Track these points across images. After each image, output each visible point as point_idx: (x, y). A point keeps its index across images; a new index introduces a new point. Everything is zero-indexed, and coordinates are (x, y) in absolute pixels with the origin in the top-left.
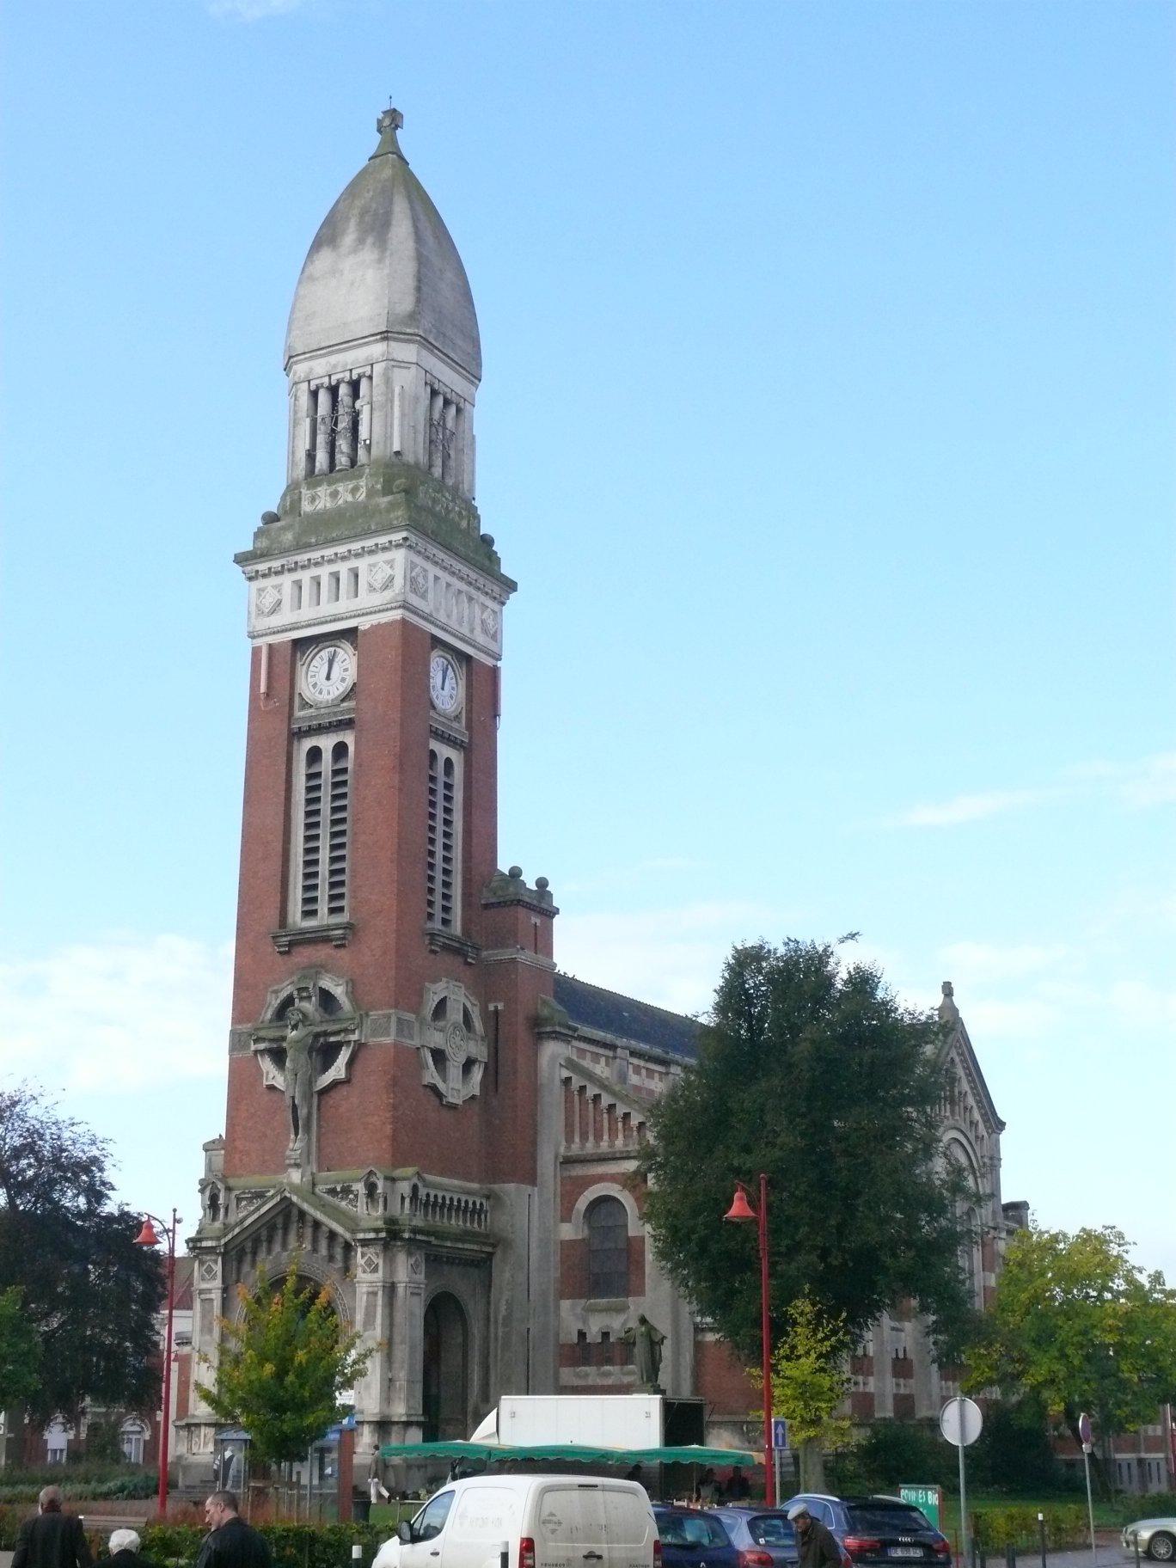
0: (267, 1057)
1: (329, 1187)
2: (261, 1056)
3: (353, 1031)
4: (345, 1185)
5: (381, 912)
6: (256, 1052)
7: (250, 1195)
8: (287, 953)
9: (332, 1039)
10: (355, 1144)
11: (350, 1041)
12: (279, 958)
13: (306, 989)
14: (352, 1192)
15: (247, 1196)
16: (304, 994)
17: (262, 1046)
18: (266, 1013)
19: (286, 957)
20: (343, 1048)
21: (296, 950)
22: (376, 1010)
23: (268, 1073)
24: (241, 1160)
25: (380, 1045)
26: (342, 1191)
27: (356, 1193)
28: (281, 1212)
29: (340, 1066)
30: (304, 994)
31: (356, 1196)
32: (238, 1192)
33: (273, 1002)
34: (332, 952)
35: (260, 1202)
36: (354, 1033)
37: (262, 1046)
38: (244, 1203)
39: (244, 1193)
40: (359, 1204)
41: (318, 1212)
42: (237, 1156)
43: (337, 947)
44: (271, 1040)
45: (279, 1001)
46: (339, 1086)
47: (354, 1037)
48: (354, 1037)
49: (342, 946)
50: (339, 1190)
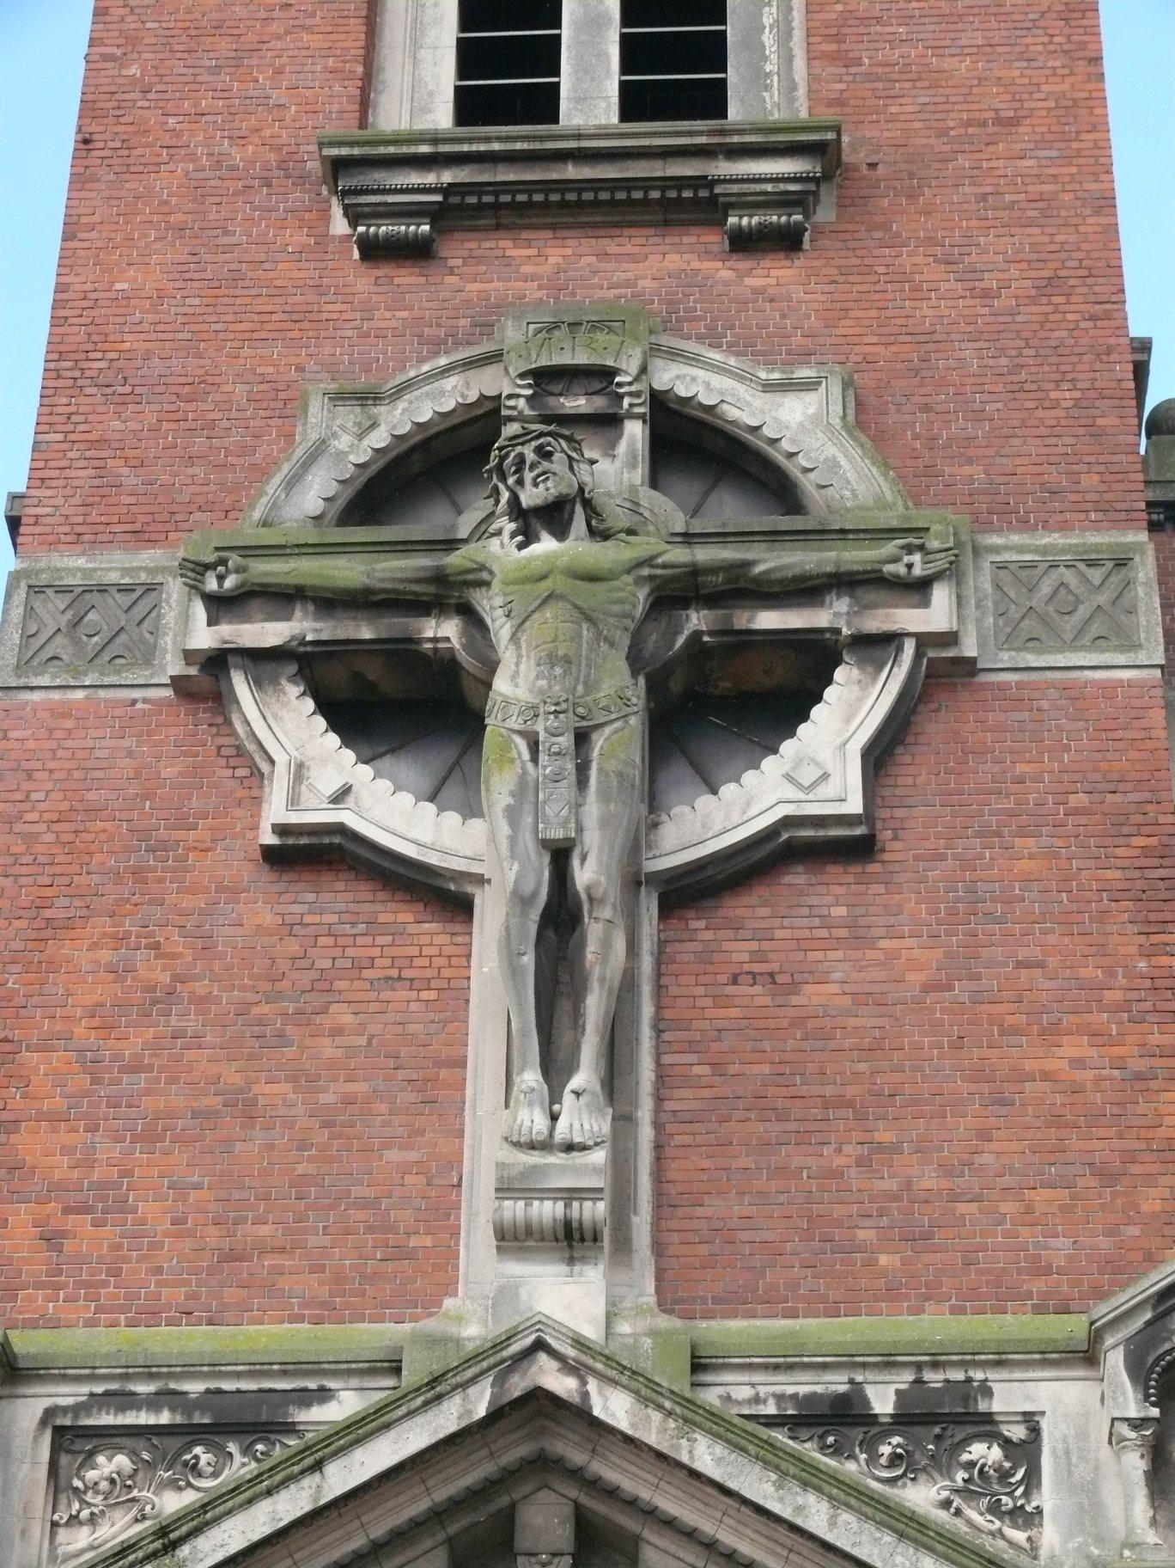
0: (293, 690)
1: (803, 1385)
2: (258, 683)
3: (919, 589)
4: (934, 1378)
5: (1013, 122)
6: (217, 662)
7: (165, 1418)
8: (416, 252)
9: (769, 620)
10: (929, 1179)
11: (889, 641)
12: (363, 281)
13: (602, 376)
14: (986, 1428)
15: (144, 1418)
16: (577, 403)
17: (269, 632)
18: (292, 482)
19: (406, 277)
20: (840, 674)
21: (456, 250)
22: (1025, 525)
23: (299, 771)
24: (52, 1239)
25: (1075, 695)
26: (903, 1420)
27: (1017, 1432)
28: (438, 1515)
29: (826, 756)
30: (577, 403)
31: (1026, 1452)
32: (67, 1395)
33: (343, 442)
34: (724, 272)
35: (240, 1466)
36: (926, 603)
37: (269, 632)
38: (111, 1464)
39: (126, 1401)
40: (1047, 1498)
41: (811, 1498)
42: (22, 1216)
43: (744, 243)
44: (329, 601)
45: (379, 438)
46: (796, 877)
47: (909, 619)
48: (937, 614)
49: (787, 241)
50: (882, 1402)
